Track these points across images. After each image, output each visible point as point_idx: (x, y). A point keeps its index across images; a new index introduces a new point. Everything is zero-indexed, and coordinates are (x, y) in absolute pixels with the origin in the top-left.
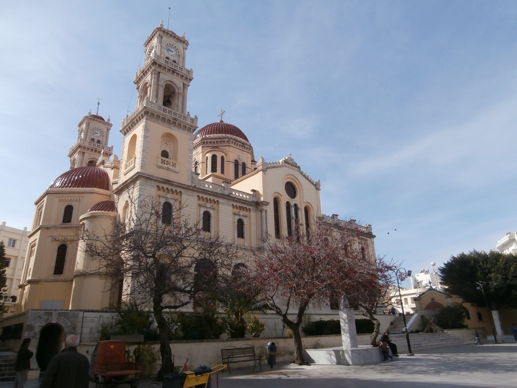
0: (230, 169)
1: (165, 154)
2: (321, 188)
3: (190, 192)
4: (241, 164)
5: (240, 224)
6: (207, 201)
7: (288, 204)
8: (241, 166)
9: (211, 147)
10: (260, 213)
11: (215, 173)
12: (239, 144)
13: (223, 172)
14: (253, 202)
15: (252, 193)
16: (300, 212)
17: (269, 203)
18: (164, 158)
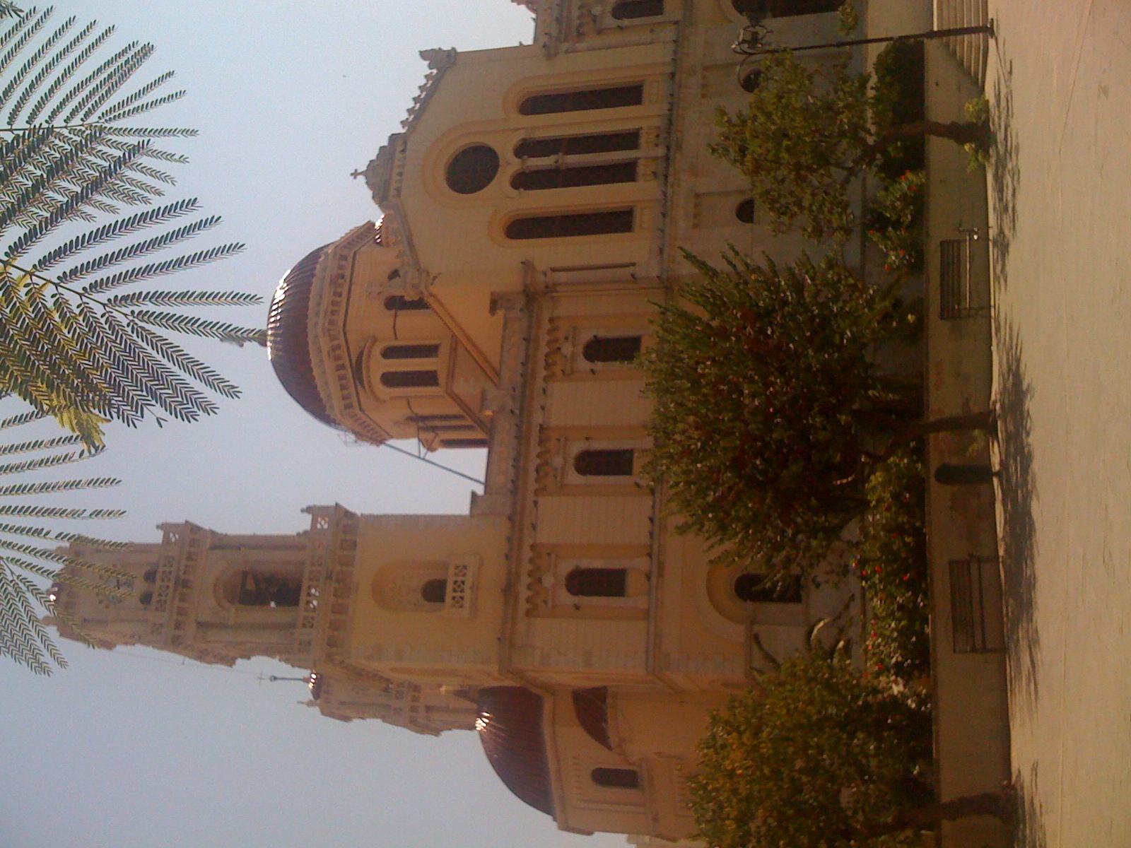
1: (434, 592)
9: (359, 387)
11: (442, 378)
13: (431, 351)
15: (500, 313)
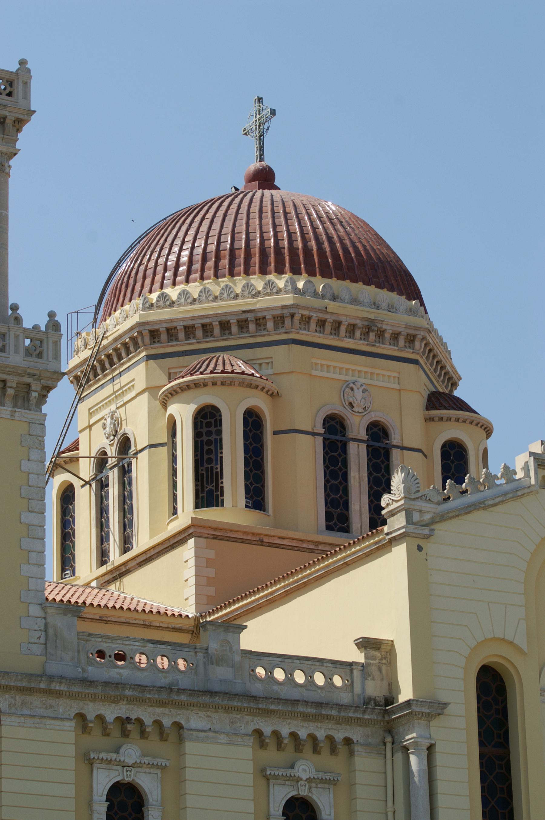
14: (370, 703)
15: (359, 657)
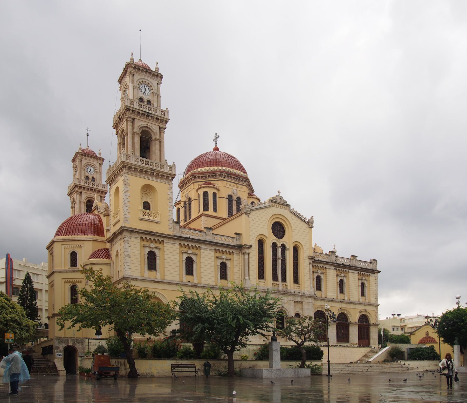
0: (223, 205)
1: (146, 206)
2: (314, 225)
3: (171, 241)
4: (236, 199)
5: (223, 267)
6: (189, 248)
7: (274, 245)
8: (236, 202)
10: (243, 255)
11: (206, 212)
12: (233, 177)
13: (215, 210)
16: (287, 252)
17: (251, 246)
18: (145, 211)
